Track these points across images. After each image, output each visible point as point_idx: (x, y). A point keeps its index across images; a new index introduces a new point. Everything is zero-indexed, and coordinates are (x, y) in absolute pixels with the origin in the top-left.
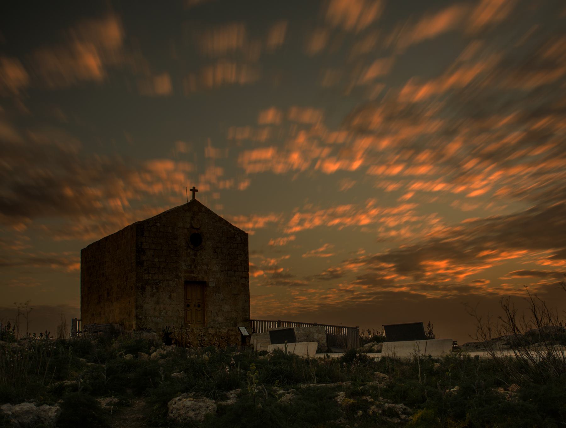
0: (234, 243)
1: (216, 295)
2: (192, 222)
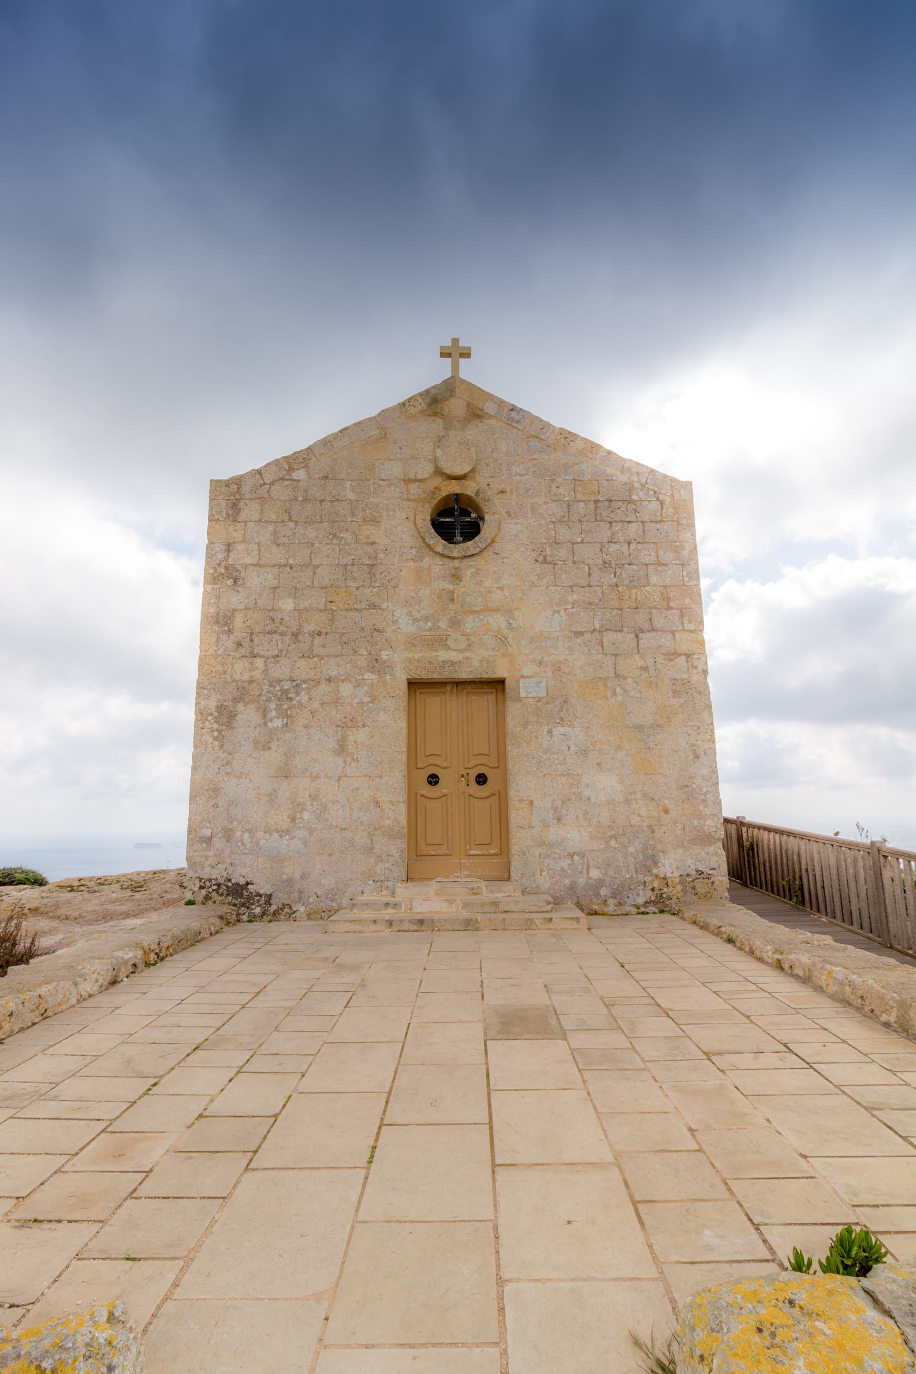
0: (629, 522)
1: (550, 732)
2: (439, 453)
